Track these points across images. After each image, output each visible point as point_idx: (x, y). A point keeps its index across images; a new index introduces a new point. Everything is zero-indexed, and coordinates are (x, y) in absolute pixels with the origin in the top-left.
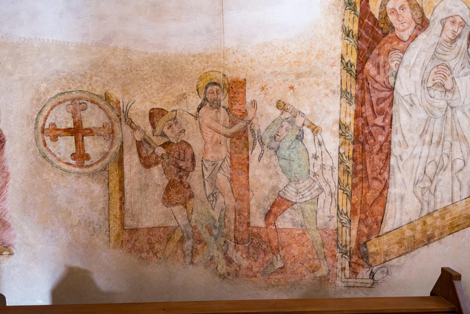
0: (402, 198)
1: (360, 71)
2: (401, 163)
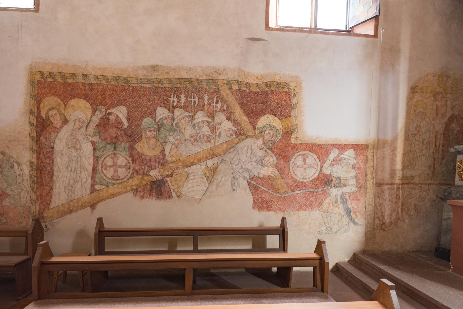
0: (59, 194)
1: (38, 140)
2: (58, 179)
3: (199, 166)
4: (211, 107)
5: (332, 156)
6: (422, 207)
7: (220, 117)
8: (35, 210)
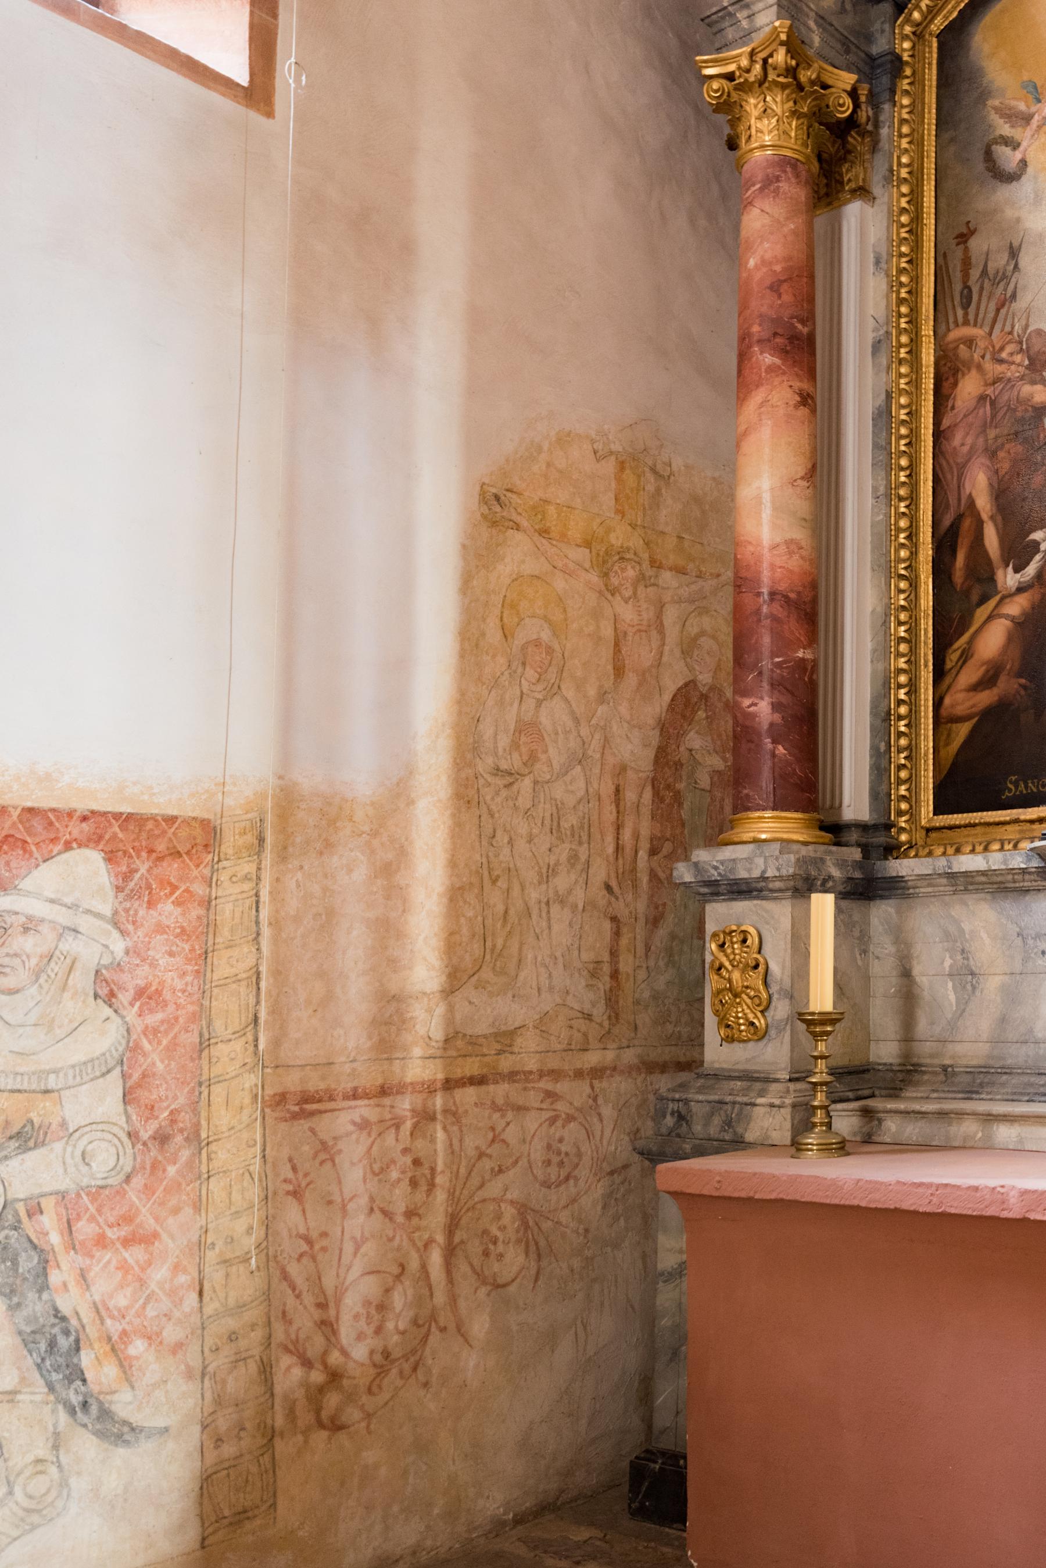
6: (564, 1216)
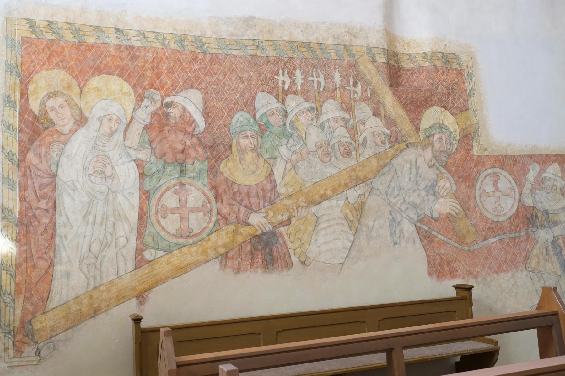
0: (68, 274)
2: (66, 243)
3: (335, 201)
4: (347, 92)
5: (532, 175)
7: (364, 110)
8: (12, 318)
